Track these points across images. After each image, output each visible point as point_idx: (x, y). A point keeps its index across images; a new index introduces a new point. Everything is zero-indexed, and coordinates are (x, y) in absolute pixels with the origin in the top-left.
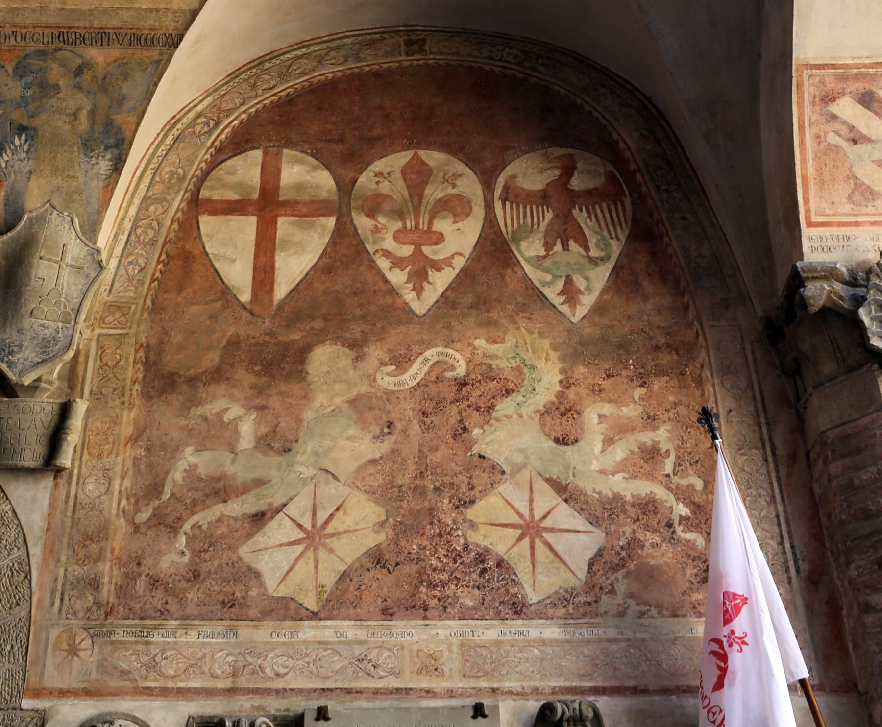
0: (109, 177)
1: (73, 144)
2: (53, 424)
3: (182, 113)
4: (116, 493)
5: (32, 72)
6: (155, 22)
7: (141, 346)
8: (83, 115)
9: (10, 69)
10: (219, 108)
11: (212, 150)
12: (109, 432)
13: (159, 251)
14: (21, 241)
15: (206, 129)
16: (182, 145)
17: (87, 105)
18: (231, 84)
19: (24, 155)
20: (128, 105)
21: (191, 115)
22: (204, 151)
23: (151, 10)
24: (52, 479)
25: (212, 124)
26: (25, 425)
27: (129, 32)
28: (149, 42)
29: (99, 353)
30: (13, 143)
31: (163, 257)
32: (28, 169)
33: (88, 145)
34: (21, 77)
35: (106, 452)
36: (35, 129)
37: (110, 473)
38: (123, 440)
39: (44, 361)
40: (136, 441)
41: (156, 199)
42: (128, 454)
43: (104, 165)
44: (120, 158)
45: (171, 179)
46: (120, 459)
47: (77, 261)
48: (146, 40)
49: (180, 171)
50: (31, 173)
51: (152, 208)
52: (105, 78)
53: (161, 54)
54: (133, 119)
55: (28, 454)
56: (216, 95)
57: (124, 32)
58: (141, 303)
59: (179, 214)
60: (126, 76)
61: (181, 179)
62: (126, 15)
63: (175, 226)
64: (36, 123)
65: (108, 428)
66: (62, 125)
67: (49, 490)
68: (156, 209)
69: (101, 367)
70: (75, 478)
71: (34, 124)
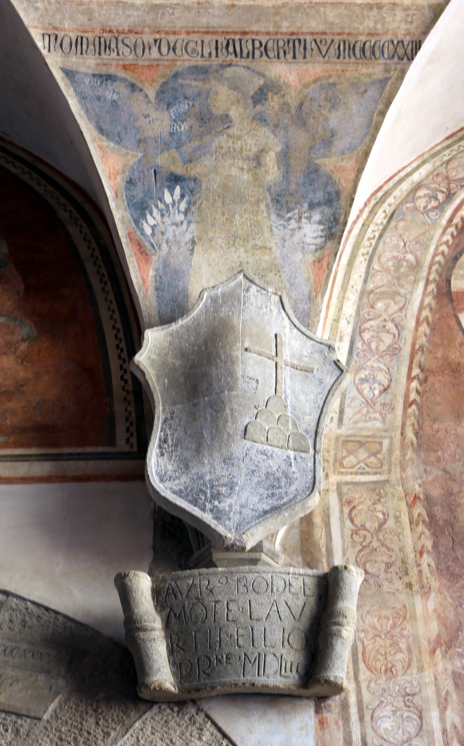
0: (321, 248)
1: (258, 201)
2: (307, 611)
3: (391, 184)
4: (438, 735)
5: (186, 98)
6: (376, 23)
7: (416, 498)
8: (270, 159)
9: (152, 94)
10: (447, 178)
11: (452, 229)
12: (397, 631)
13: (406, 363)
14: (204, 330)
15: (434, 203)
16: (401, 224)
17: (275, 145)
18: (455, 147)
19: (181, 217)
20: (340, 144)
21: (405, 186)
22: (440, 231)
23: (370, 7)
24: (312, 711)
25: (441, 197)
26: (260, 611)
27: (337, 38)
28: (368, 53)
29: (346, 510)
30: (161, 200)
31: (416, 371)
32: (188, 236)
33: (282, 201)
34: (169, 105)
35: (399, 666)
36: (195, 180)
37: (416, 700)
38: (425, 644)
39: (275, 509)
40: (449, 645)
41: (382, 293)
42: (440, 667)
43: (311, 231)
44: (336, 220)
45: (398, 266)
46: (428, 676)
47: (300, 359)
48: (363, 50)
49: (410, 257)
50: (193, 242)
51: (380, 305)
52: (301, 105)
53: (387, 70)
54: (350, 164)
55: (272, 664)
56: (437, 161)
57: (329, 38)
58: (398, 435)
59: (426, 313)
60: (334, 103)
61: (416, 267)
62: (331, 15)
63: (424, 328)
64: (196, 170)
65: (394, 626)
66: (237, 172)
67: (312, 732)
68: (387, 306)
69: (355, 532)
70: (353, 710)
71: (193, 173)
